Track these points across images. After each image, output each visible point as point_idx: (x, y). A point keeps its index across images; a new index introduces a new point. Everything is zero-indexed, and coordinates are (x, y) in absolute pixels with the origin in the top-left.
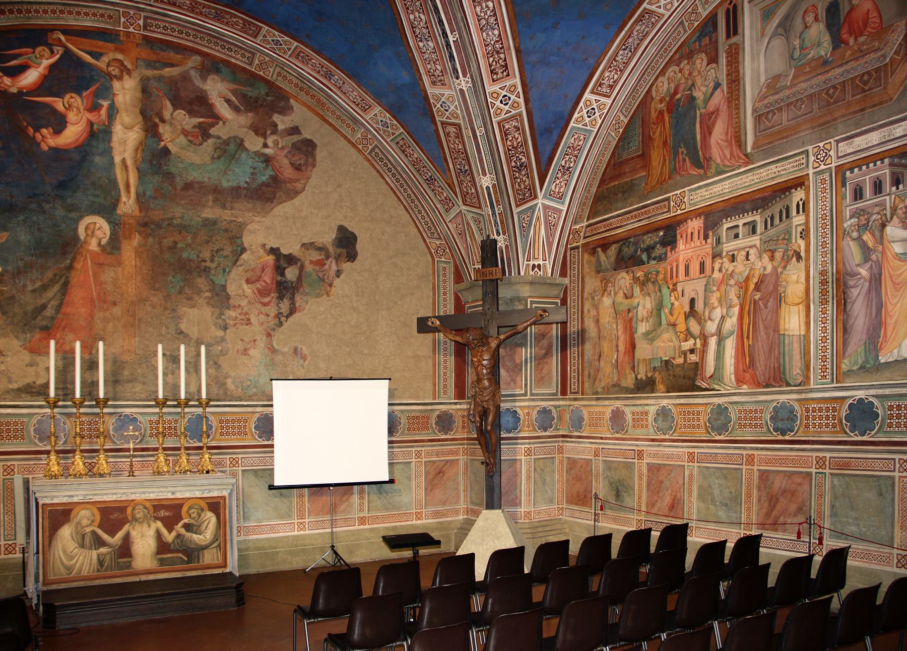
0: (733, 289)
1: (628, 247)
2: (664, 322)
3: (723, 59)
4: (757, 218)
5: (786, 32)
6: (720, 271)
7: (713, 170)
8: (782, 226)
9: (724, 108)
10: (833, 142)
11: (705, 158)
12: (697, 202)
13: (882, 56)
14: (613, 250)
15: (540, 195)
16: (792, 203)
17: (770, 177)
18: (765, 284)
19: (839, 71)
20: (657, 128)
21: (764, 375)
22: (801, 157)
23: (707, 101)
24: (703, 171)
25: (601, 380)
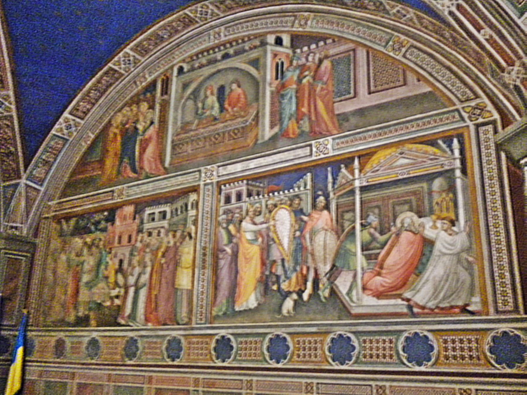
3: (158, 107)
6: (141, 241)
9: (155, 137)
14: (73, 222)
15: (24, 176)
23: (144, 131)
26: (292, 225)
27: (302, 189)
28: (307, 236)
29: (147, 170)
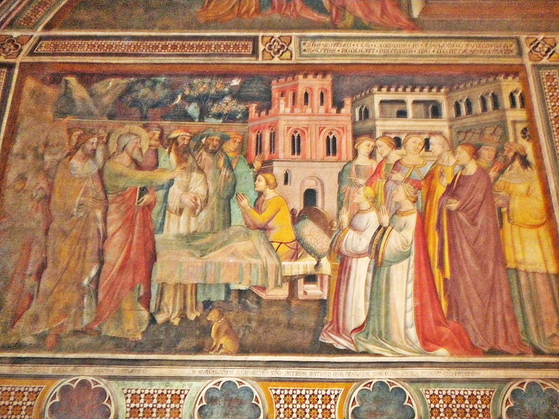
1: (152, 88)
2: (237, 219)
6: (372, 155)
8: (486, 117)
21: (483, 332)
25: (36, 319)
29: (359, 13)
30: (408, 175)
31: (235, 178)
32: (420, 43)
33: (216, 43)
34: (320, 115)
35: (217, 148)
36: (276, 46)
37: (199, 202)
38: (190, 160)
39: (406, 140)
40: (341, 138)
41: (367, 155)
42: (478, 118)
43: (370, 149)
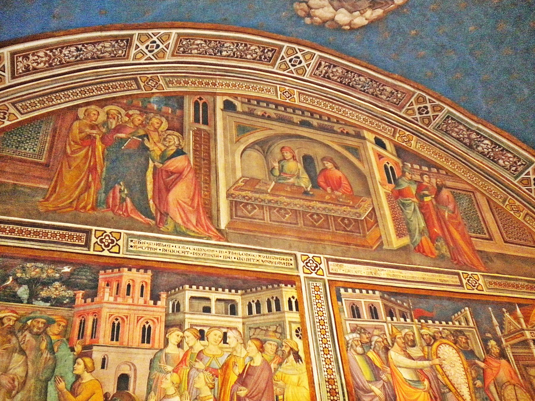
0: (201, 375)
4: (238, 298)
5: (264, 152)
6: (180, 345)
7: (170, 226)
8: (270, 316)
10: (322, 258)
11: (157, 209)
12: (140, 252)
13: (357, 213)
16: (282, 297)
17: (252, 262)
18: (255, 377)
19: (319, 205)
20: (81, 149)
22: (289, 257)
23: (164, 158)
24: (154, 222)
26: (466, 370)
27: (463, 324)
28: (492, 388)
29: (180, 221)
30: (208, 364)
31: (55, 359)
32: (224, 250)
33: (53, 231)
34: (139, 305)
35: (42, 330)
36: (107, 241)
37: (16, 383)
38: (14, 340)
39: (209, 333)
40: (156, 328)
41: (177, 344)
42: (265, 317)
43: (179, 339)
